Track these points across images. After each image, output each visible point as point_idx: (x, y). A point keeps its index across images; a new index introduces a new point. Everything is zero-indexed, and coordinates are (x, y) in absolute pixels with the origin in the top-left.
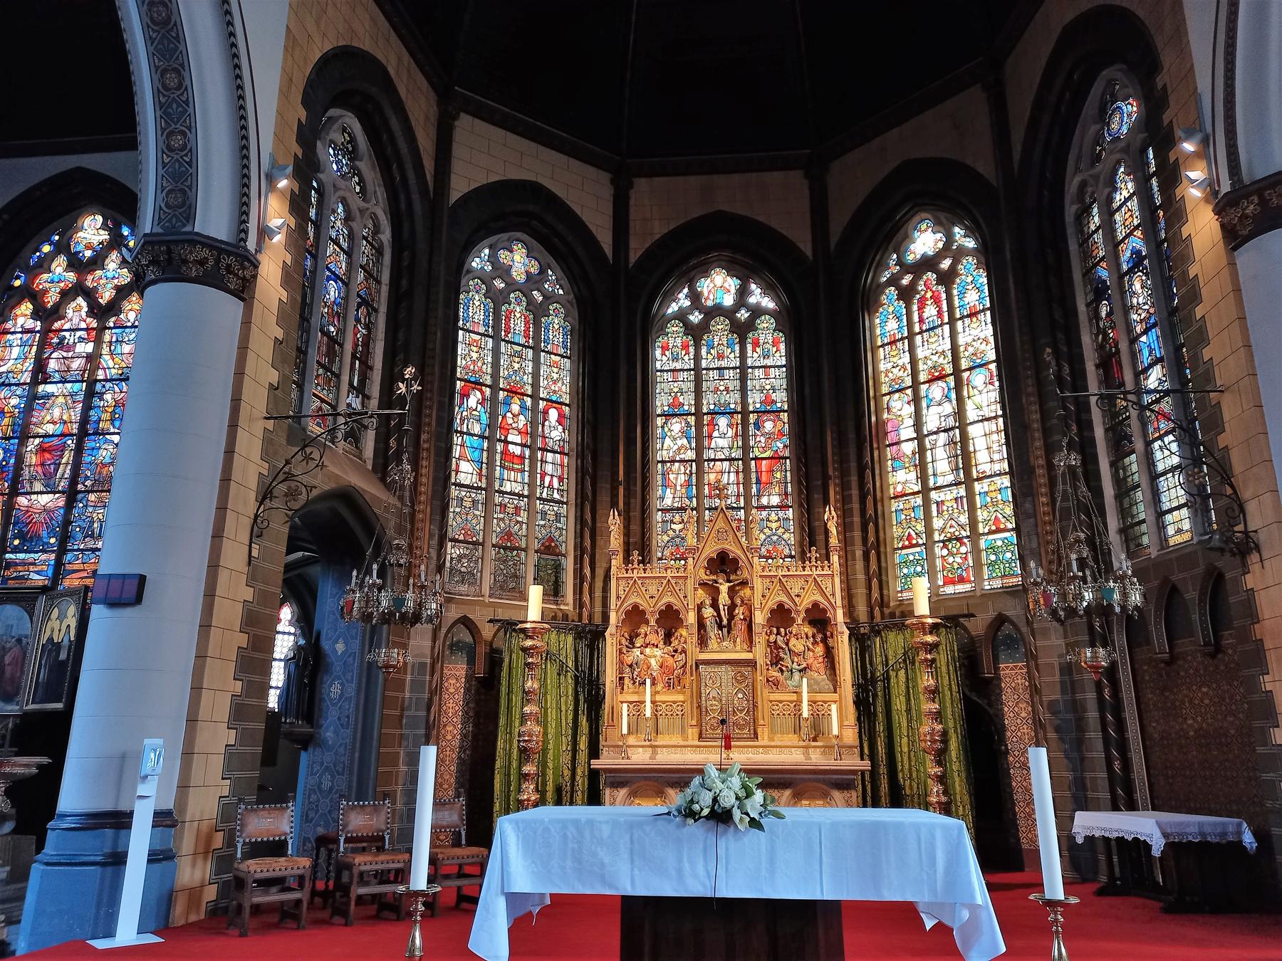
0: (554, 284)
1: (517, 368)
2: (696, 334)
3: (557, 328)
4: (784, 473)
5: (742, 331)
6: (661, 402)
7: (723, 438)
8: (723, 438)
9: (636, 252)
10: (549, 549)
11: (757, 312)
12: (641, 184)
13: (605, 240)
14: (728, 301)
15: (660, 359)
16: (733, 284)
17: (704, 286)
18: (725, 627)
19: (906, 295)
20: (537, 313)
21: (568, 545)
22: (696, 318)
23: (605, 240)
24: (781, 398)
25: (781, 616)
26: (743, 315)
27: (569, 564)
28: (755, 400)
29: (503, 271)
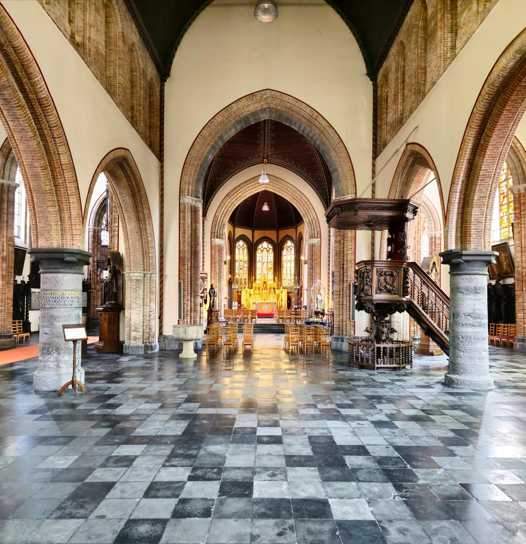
0: (245, 246)
1: (241, 258)
2: (262, 251)
3: (246, 251)
4: (272, 270)
5: (268, 251)
6: (257, 260)
7: (265, 266)
8: (265, 266)
9: (255, 241)
10: (245, 279)
11: (270, 249)
12: (256, 231)
13: (251, 240)
14: (266, 247)
15: (258, 255)
16: (267, 244)
17: (263, 244)
18: (265, 289)
19: (287, 250)
20: (243, 250)
21: (247, 278)
22: (262, 249)
23: (251, 240)
24: (272, 261)
25: (270, 288)
26: (268, 249)
27: (247, 281)
28: (269, 261)
29: (239, 245)
